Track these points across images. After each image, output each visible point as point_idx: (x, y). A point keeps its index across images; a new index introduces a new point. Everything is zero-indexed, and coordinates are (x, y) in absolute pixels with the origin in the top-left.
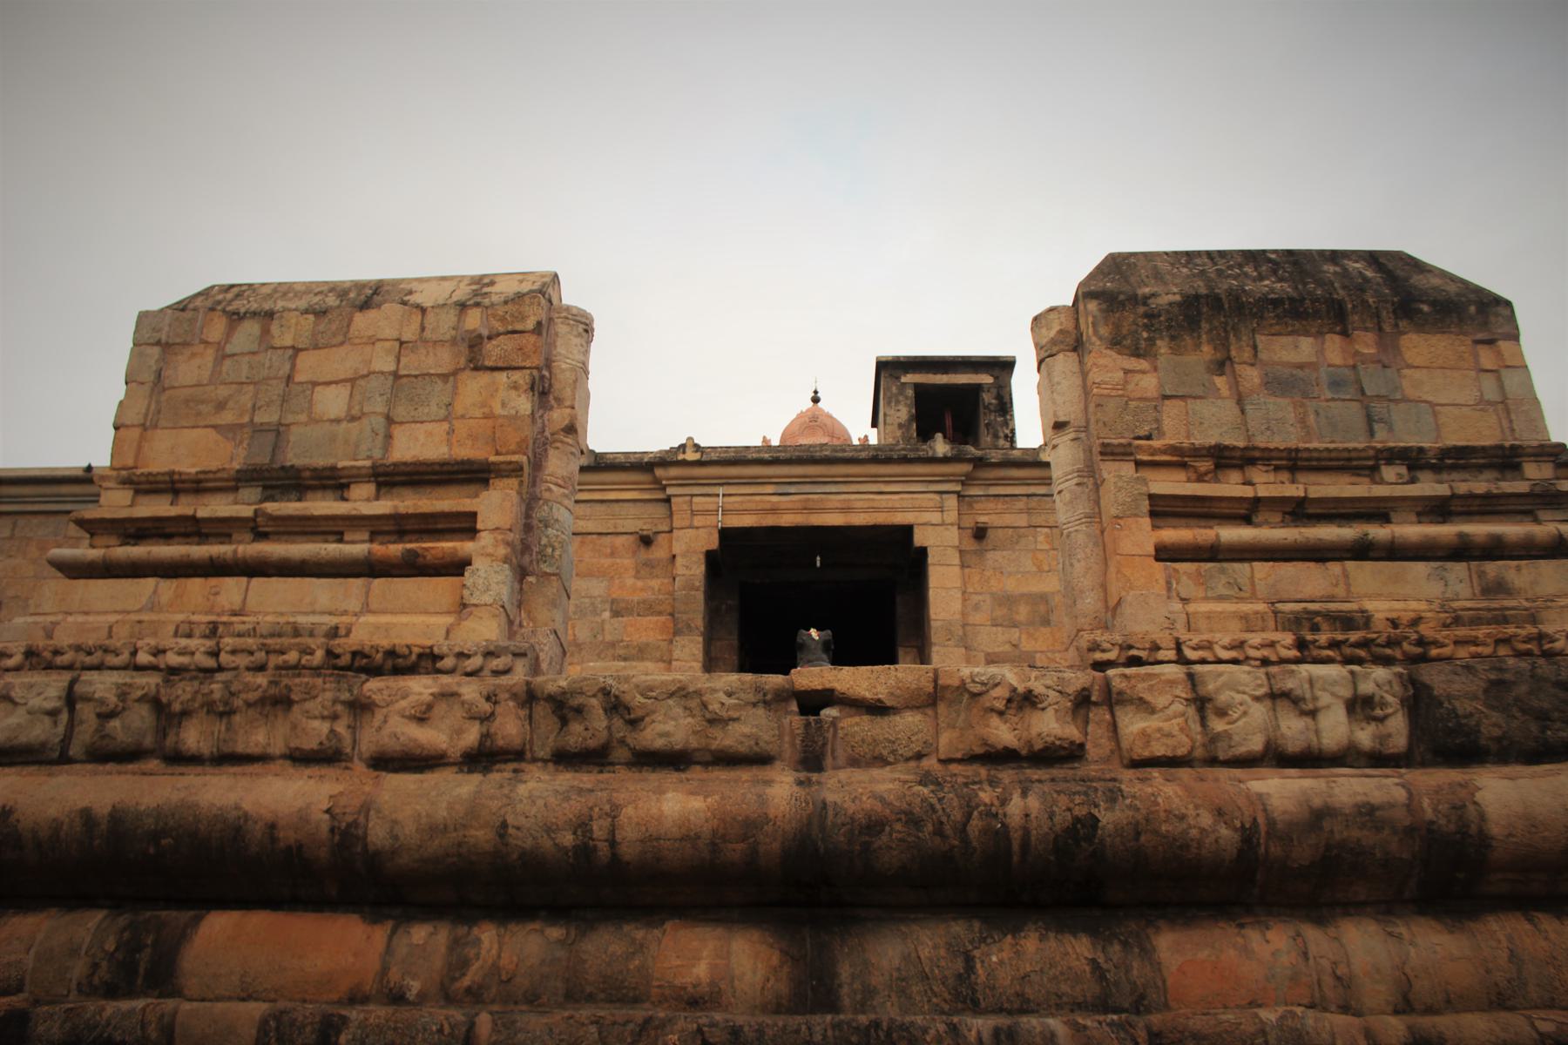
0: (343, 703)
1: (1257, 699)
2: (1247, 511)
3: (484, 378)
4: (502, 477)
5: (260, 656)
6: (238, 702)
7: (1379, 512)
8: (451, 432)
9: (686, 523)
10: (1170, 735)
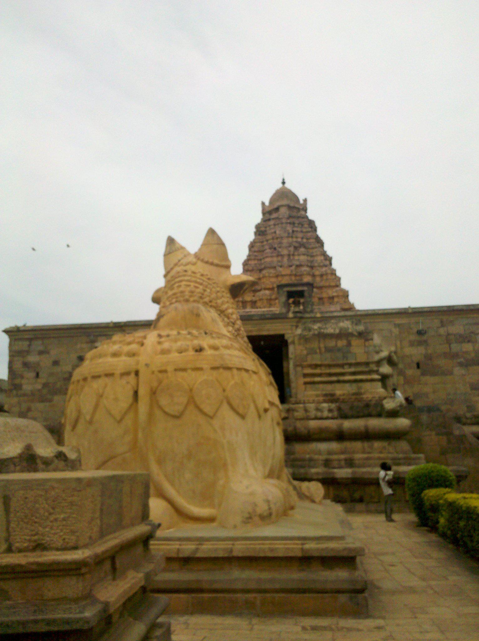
2: (320, 375)
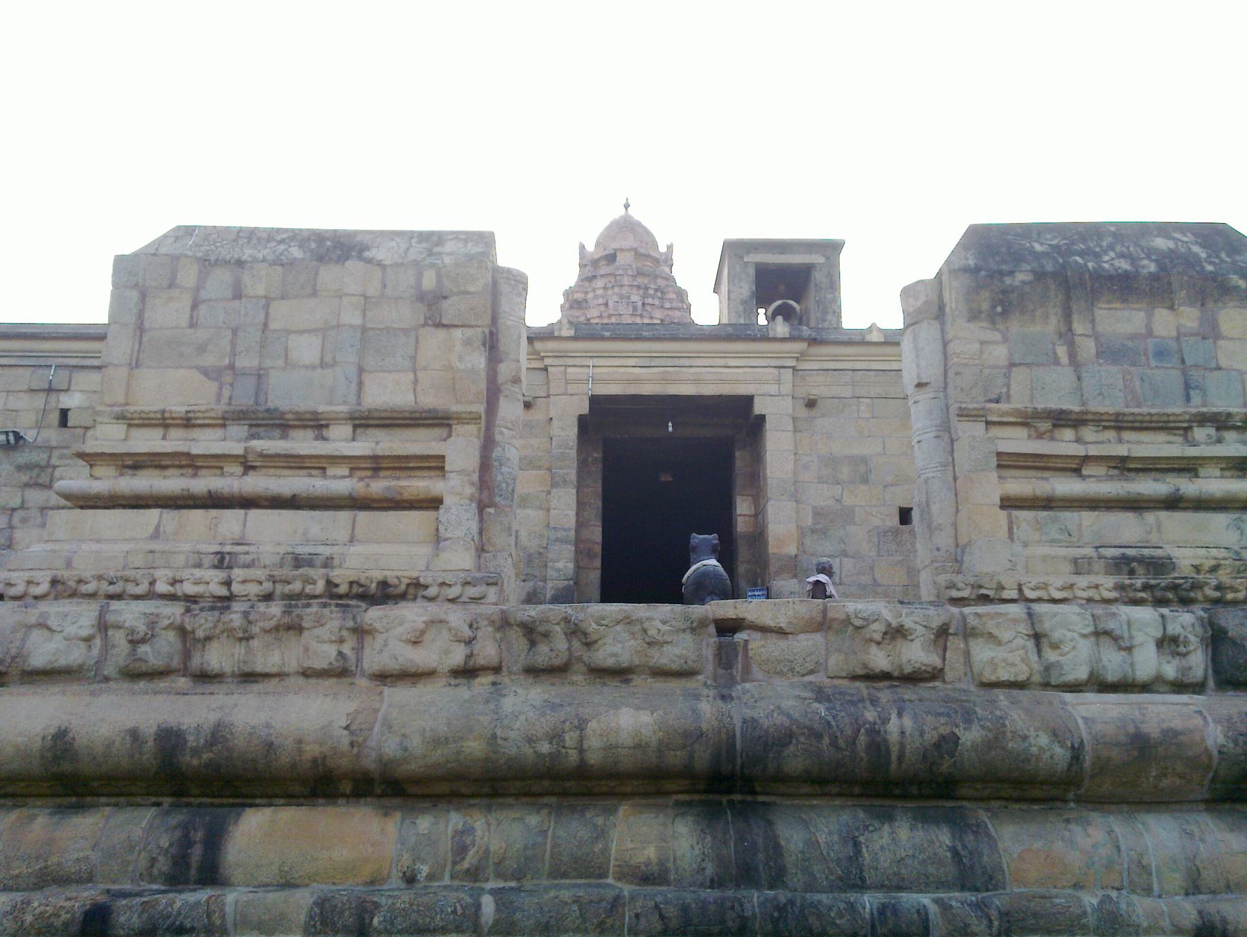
0: (348, 629)
1: (1084, 636)
2: (1075, 467)
3: (441, 334)
4: (463, 423)
5: (268, 586)
6: (255, 629)
7: (1189, 467)
8: (416, 382)
9: (561, 390)
10: (1013, 665)
